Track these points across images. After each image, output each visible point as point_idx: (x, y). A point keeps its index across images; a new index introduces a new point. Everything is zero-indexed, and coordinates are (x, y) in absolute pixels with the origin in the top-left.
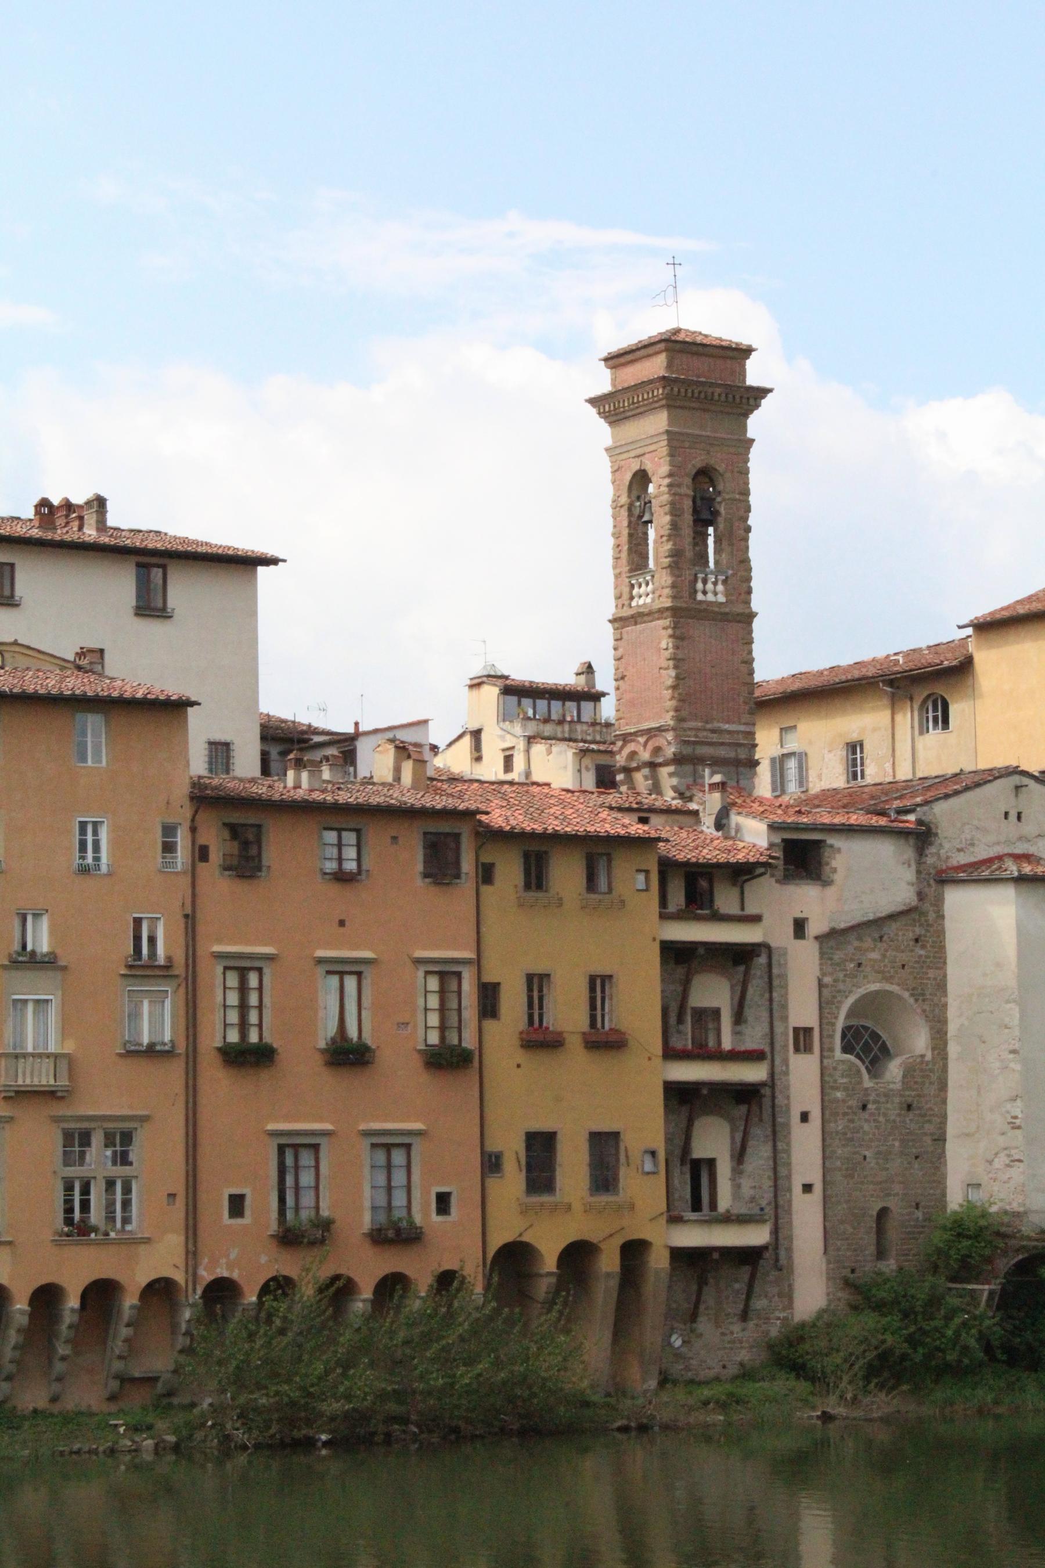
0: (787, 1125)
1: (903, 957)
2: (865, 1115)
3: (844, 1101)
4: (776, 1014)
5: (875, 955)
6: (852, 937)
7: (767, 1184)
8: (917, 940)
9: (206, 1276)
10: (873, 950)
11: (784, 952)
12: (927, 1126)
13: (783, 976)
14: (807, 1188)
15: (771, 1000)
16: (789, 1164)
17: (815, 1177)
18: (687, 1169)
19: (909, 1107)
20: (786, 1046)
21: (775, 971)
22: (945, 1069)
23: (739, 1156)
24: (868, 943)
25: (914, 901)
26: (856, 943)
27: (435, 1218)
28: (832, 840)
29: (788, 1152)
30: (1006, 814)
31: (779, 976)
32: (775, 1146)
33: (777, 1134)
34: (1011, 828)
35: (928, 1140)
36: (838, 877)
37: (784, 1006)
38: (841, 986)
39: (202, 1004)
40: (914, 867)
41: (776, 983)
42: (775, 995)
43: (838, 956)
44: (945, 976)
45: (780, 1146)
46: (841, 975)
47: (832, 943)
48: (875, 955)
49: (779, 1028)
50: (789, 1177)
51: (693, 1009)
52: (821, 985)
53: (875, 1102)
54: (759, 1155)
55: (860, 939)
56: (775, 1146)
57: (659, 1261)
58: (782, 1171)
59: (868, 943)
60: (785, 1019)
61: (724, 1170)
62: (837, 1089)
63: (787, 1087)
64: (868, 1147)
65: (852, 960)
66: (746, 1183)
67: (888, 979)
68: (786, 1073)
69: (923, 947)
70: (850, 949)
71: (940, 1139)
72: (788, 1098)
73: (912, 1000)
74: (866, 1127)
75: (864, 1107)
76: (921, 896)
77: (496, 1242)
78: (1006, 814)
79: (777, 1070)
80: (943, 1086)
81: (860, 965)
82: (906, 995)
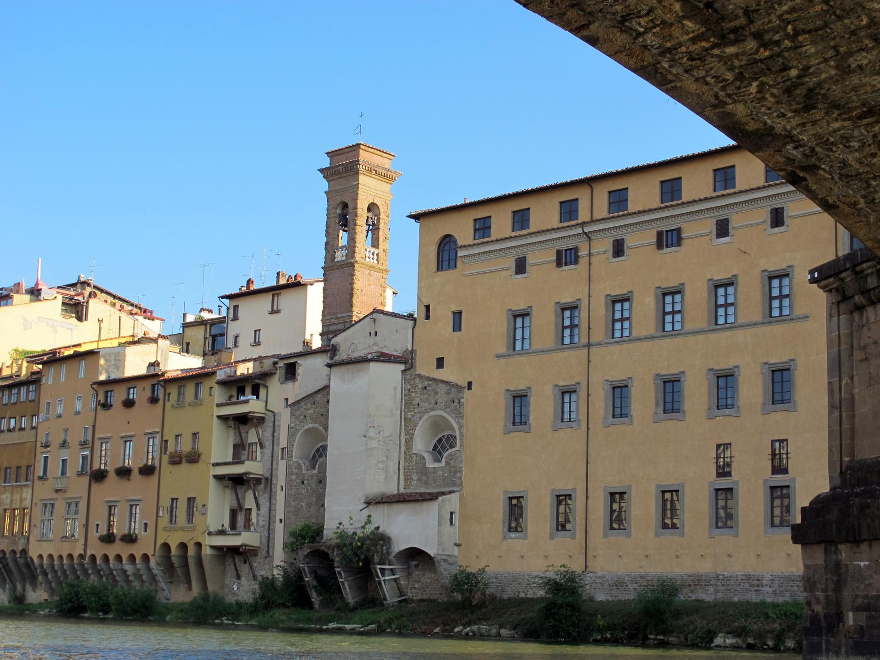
2: (303, 486)
5: (311, 411)
6: (302, 404)
9: (89, 553)
10: (309, 409)
15: (273, 436)
18: (243, 513)
21: (277, 423)
27: (143, 533)
29: (275, 504)
34: (373, 339)
36: (299, 378)
37: (278, 439)
39: (95, 456)
41: (276, 429)
43: (298, 413)
45: (273, 501)
51: (249, 444)
55: (306, 405)
57: (207, 551)
58: (273, 513)
59: (309, 405)
60: (278, 444)
61: (254, 512)
66: (261, 519)
67: (315, 422)
75: (303, 483)
77: (160, 542)
79: (274, 467)
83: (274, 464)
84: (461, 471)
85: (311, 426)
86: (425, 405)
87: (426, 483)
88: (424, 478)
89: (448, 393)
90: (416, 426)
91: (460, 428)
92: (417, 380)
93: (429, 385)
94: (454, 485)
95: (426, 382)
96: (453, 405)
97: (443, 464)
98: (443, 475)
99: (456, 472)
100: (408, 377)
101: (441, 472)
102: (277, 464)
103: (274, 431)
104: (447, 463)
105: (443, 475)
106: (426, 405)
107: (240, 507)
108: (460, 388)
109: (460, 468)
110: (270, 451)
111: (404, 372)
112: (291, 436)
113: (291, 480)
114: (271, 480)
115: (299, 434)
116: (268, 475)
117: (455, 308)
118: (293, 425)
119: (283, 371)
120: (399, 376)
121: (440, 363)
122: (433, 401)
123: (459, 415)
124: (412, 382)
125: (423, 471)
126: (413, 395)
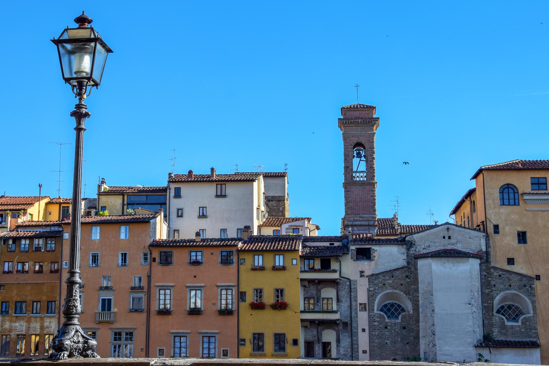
0: (357, 332)
1: (402, 282)
3: (378, 326)
4: (353, 300)
5: (390, 281)
6: (381, 276)
7: (349, 350)
8: (407, 277)
11: (356, 281)
12: (411, 334)
13: (356, 289)
14: (364, 352)
15: (351, 295)
16: (357, 344)
17: (367, 349)
19: (404, 328)
20: (356, 309)
21: (352, 287)
22: (418, 316)
23: (338, 341)
24: (387, 277)
25: (406, 264)
26: (383, 278)
28: (374, 247)
29: (357, 340)
30: (444, 237)
31: (354, 288)
32: (352, 339)
33: (353, 335)
35: (412, 338)
37: (356, 297)
38: (377, 291)
40: (405, 255)
41: (353, 290)
42: (352, 294)
44: (418, 287)
45: (354, 338)
46: (377, 288)
47: (373, 278)
48: (390, 281)
49: (354, 303)
50: (358, 348)
52: (369, 291)
53: (390, 326)
54: (346, 341)
55: (384, 276)
56: (352, 339)
58: (355, 346)
59: (387, 277)
60: (356, 301)
62: (375, 322)
63: (357, 321)
64: (388, 340)
65: (381, 283)
68: (357, 317)
69: (409, 279)
70: (380, 280)
71: (417, 338)
72: (357, 324)
73: (405, 295)
74: (387, 334)
75: (386, 328)
76: (408, 263)
78: (444, 237)
79: (353, 316)
80: (418, 321)
81: (384, 284)
82: (402, 293)
83: (353, 313)
84: (535, 329)
85: (391, 291)
86: (502, 286)
87: (505, 334)
88: (504, 331)
89: (521, 280)
90: (493, 298)
91: (533, 302)
92: (492, 270)
93: (503, 274)
94: (531, 337)
95: (500, 272)
96: (525, 289)
97: (520, 324)
98: (520, 331)
99: (531, 329)
100: (484, 267)
101: (518, 329)
102: (356, 313)
103: (351, 292)
104: (523, 323)
105: (520, 331)
106: (502, 286)
107: (319, 340)
108: (530, 278)
109: (535, 327)
110: (348, 303)
111: (480, 264)
112: (371, 296)
113: (375, 325)
114: (351, 324)
115: (380, 295)
116: (348, 320)
117: (520, 229)
118: (371, 289)
119: (355, 253)
120: (478, 267)
121: (511, 261)
122: (507, 285)
123: (531, 294)
124: (488, 271)
125: (503, 326)
126: (490, 279)
